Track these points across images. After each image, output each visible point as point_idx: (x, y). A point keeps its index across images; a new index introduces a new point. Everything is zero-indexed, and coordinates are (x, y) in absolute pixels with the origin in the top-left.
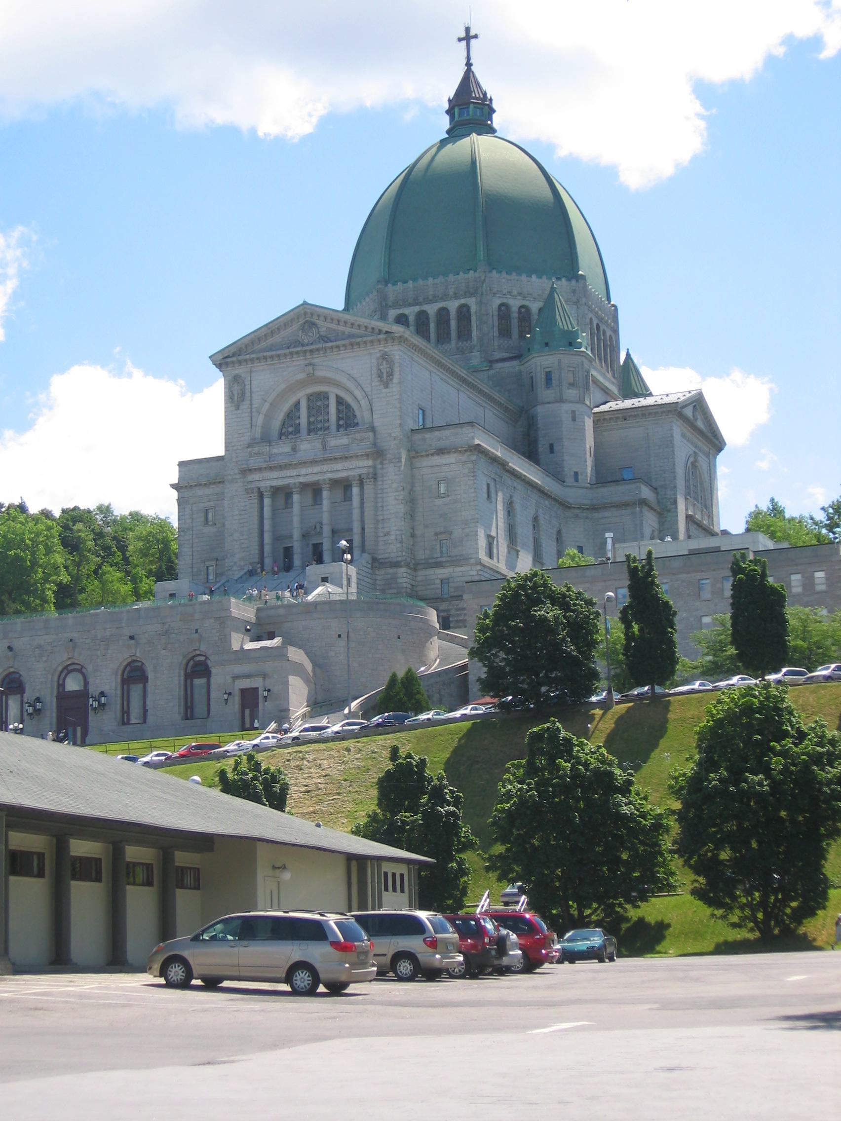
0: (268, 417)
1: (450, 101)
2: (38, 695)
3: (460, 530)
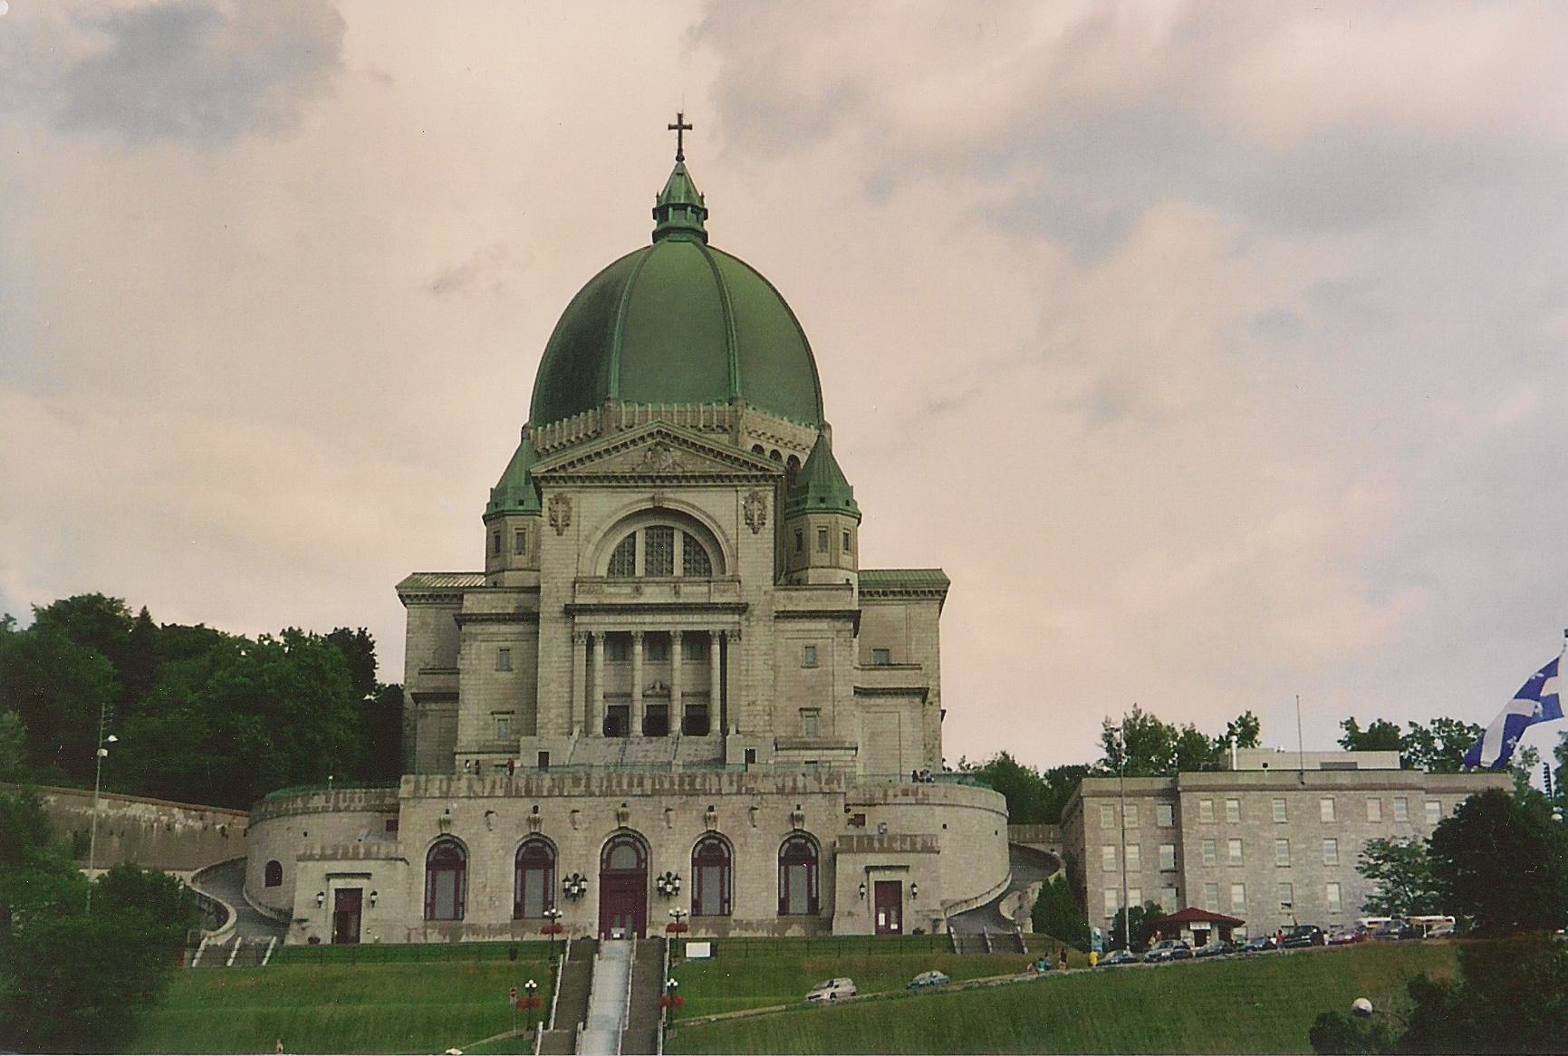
0: (599, 548)
1: (657, 196)
2: (576, 871)
3: (831, 708)
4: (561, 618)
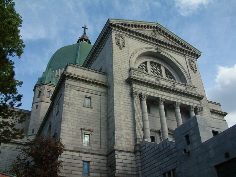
1: (80, 38)
4: (124, 84)
